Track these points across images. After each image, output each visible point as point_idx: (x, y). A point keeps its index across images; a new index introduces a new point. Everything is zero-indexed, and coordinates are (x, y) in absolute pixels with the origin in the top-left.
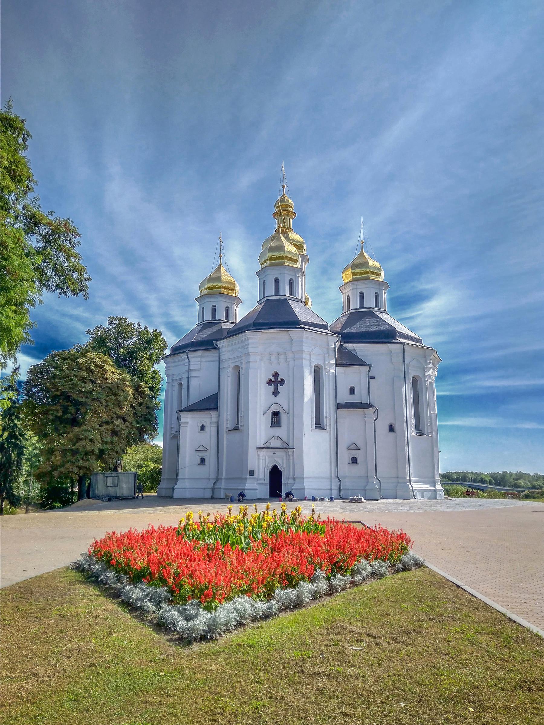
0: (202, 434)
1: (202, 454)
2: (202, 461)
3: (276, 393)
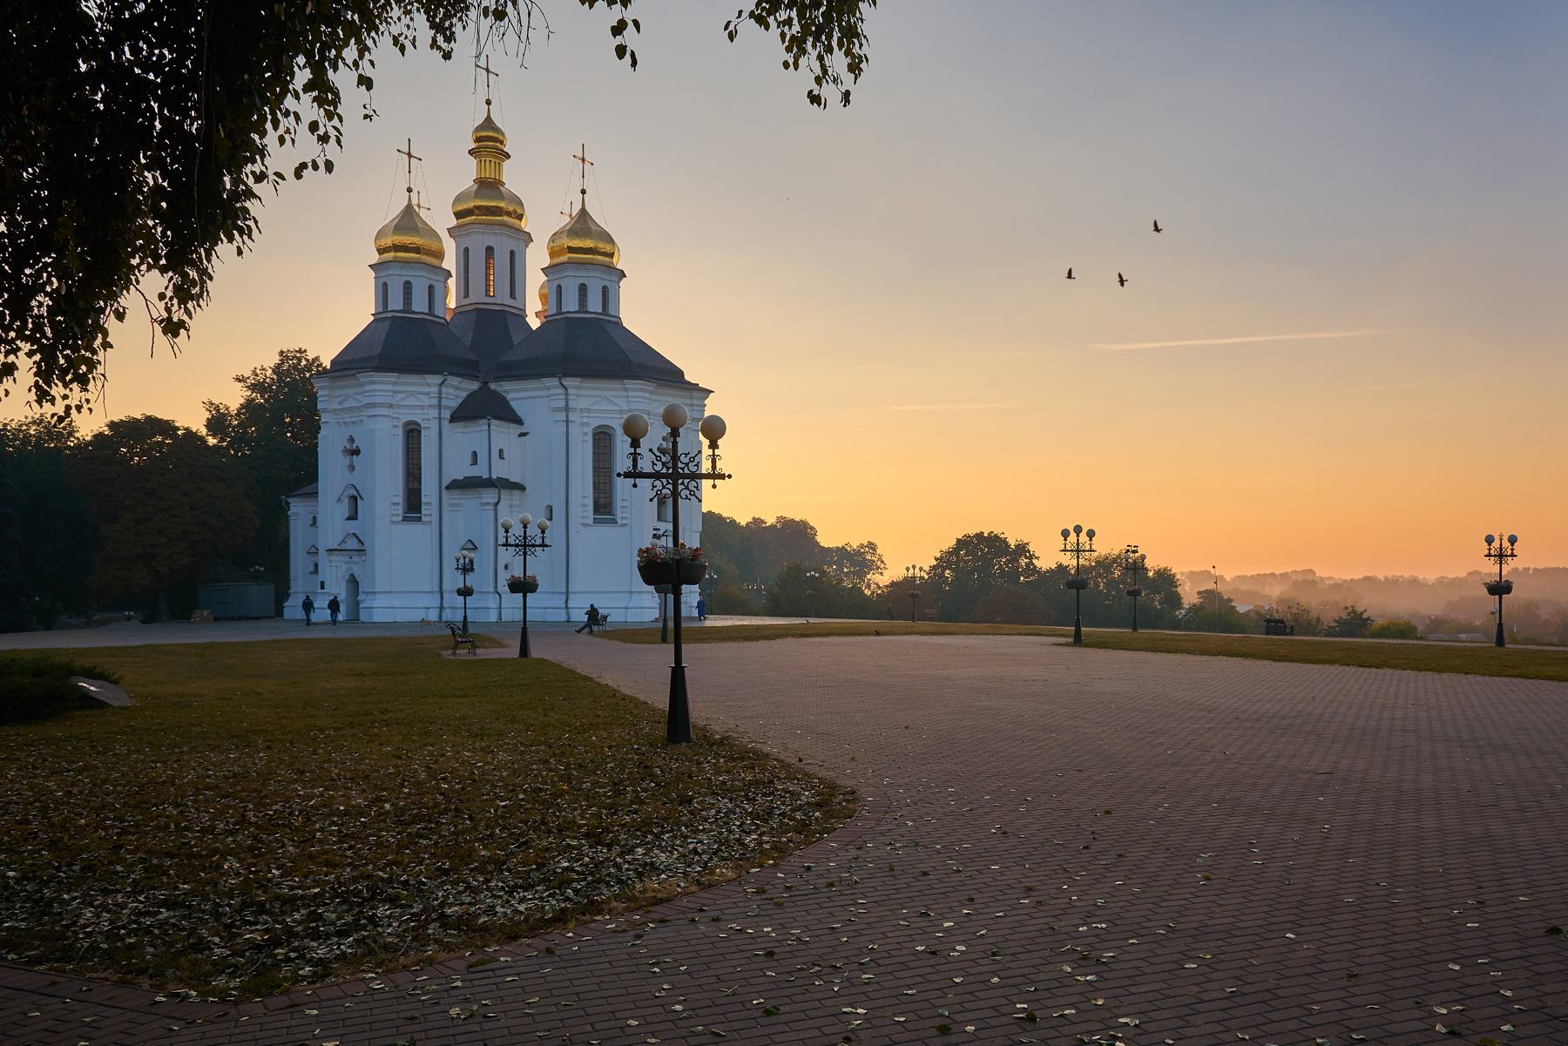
3: (352, 468)
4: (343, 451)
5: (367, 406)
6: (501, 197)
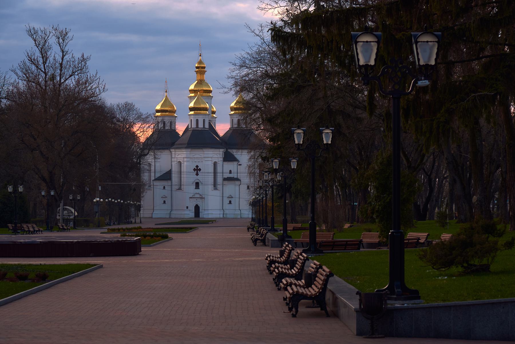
0: (164, 190)
1: (164, 199)
2: (164, 202)
3: (197, 174)
5: (205, 157)
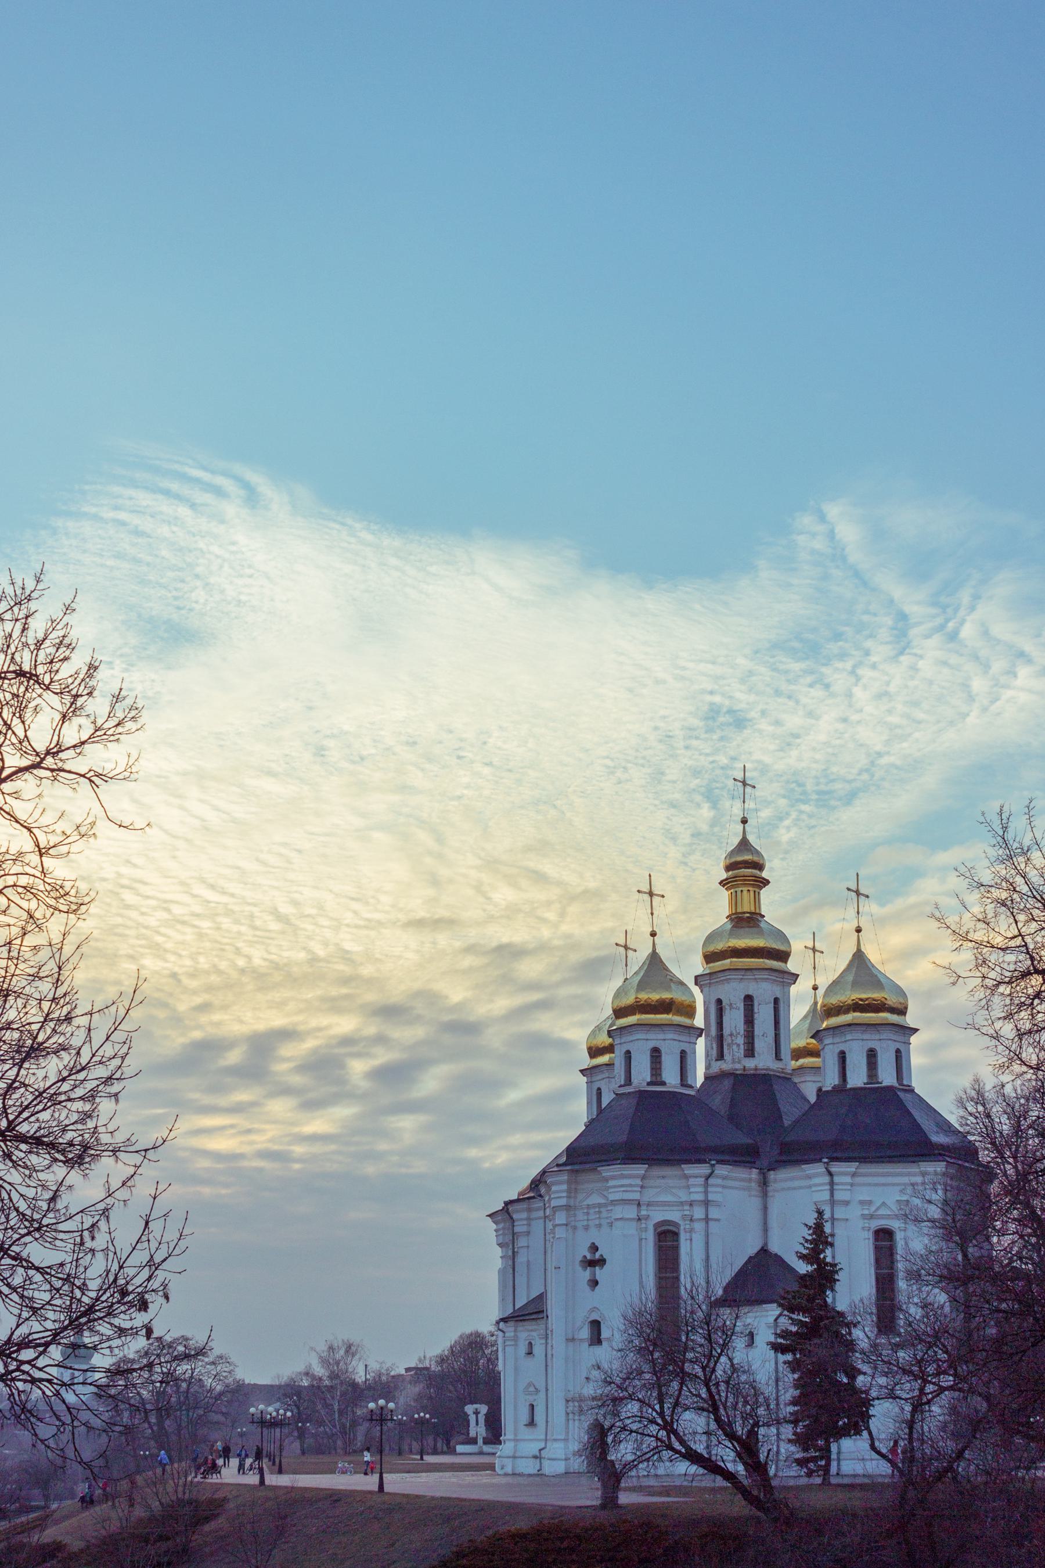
3: (594, 1283)
4: (581, 1261)
6: (761, 933)
